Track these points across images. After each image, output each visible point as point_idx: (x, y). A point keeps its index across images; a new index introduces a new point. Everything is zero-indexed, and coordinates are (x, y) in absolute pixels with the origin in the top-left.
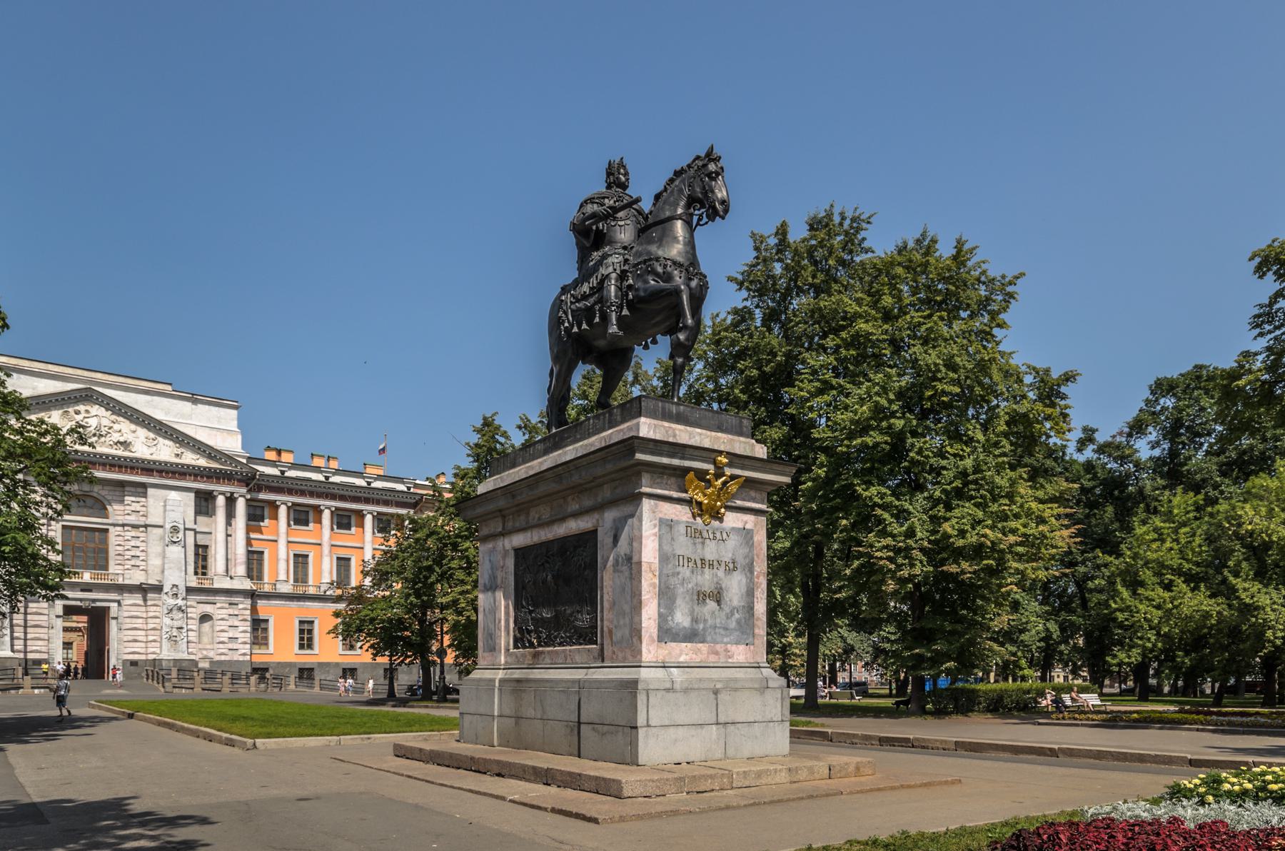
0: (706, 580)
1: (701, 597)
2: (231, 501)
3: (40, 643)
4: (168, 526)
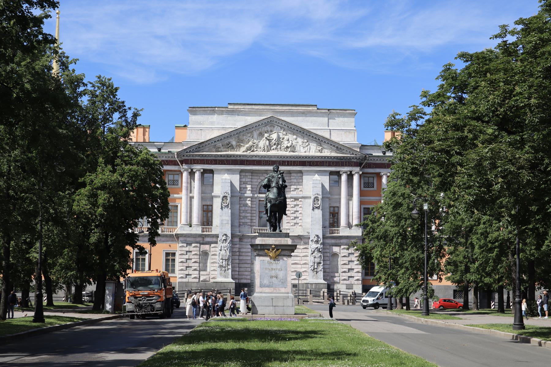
0: (273, 273)
1: (272, 277)
2: (350, 176)
3: (247, 273)
4: (313, 197)
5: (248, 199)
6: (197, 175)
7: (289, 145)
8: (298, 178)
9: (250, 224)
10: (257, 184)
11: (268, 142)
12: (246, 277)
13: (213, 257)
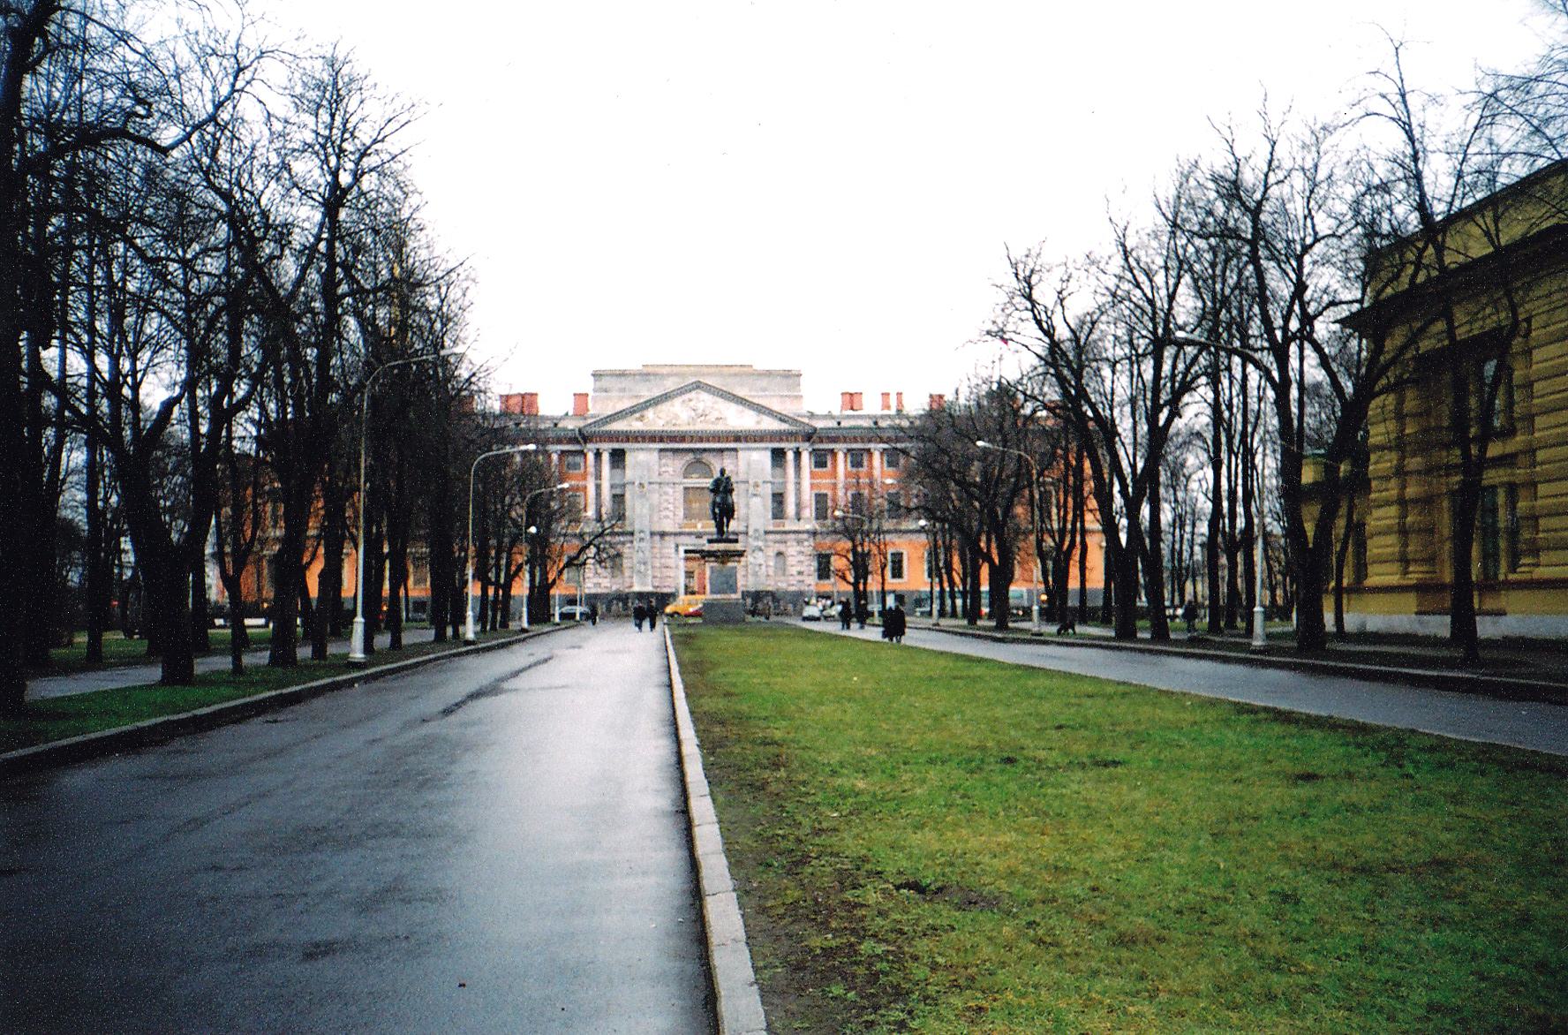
2: (798, 454)
6: (606, 457)
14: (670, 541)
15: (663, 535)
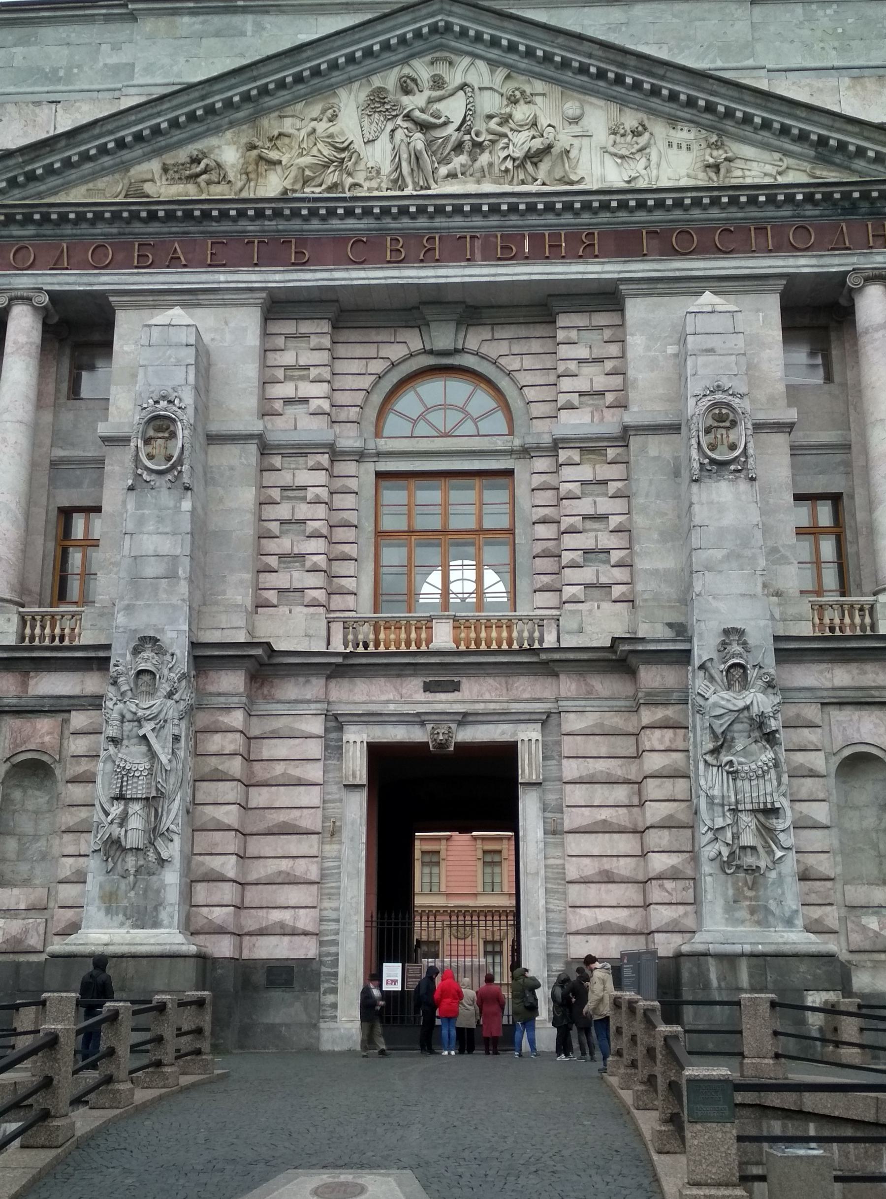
5: (311, 461)
7: (537, 144)
8: (594, 336)
9: (320, 595)
10: (366, 382)
11: (419, 141)
12: (285, 916)
13: (77, 792)
14: (301, 707)
15: (265, 666)
